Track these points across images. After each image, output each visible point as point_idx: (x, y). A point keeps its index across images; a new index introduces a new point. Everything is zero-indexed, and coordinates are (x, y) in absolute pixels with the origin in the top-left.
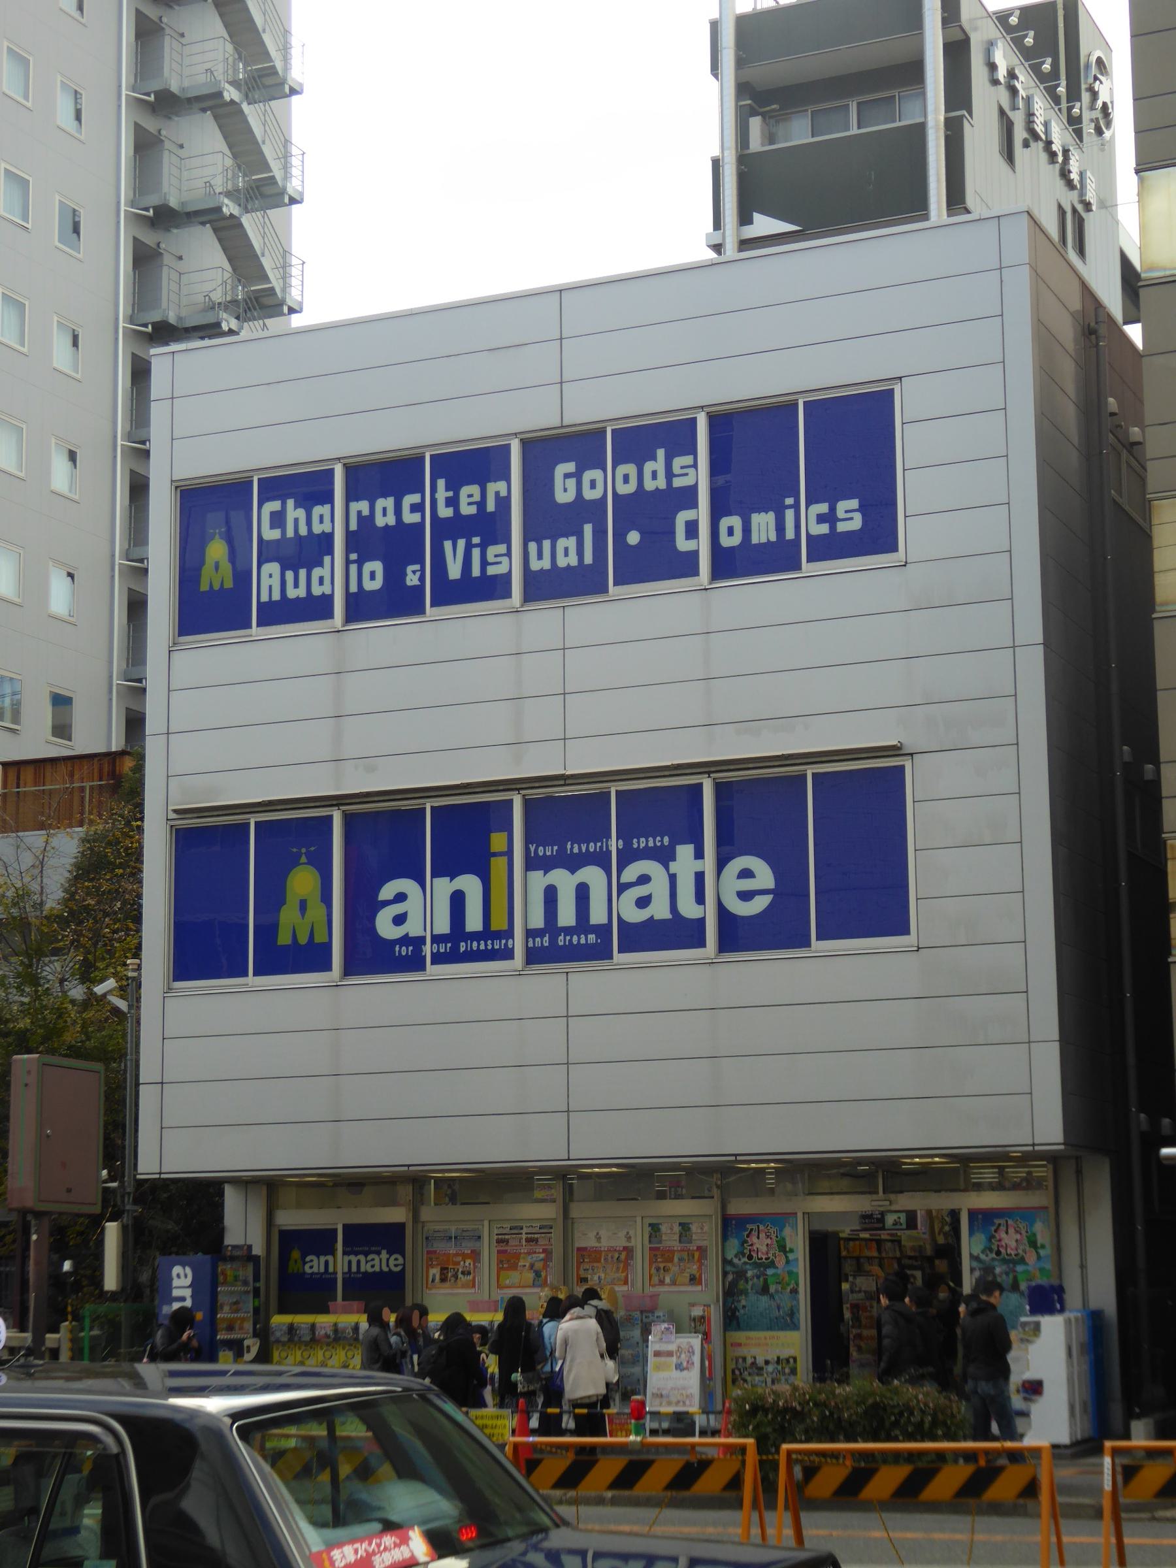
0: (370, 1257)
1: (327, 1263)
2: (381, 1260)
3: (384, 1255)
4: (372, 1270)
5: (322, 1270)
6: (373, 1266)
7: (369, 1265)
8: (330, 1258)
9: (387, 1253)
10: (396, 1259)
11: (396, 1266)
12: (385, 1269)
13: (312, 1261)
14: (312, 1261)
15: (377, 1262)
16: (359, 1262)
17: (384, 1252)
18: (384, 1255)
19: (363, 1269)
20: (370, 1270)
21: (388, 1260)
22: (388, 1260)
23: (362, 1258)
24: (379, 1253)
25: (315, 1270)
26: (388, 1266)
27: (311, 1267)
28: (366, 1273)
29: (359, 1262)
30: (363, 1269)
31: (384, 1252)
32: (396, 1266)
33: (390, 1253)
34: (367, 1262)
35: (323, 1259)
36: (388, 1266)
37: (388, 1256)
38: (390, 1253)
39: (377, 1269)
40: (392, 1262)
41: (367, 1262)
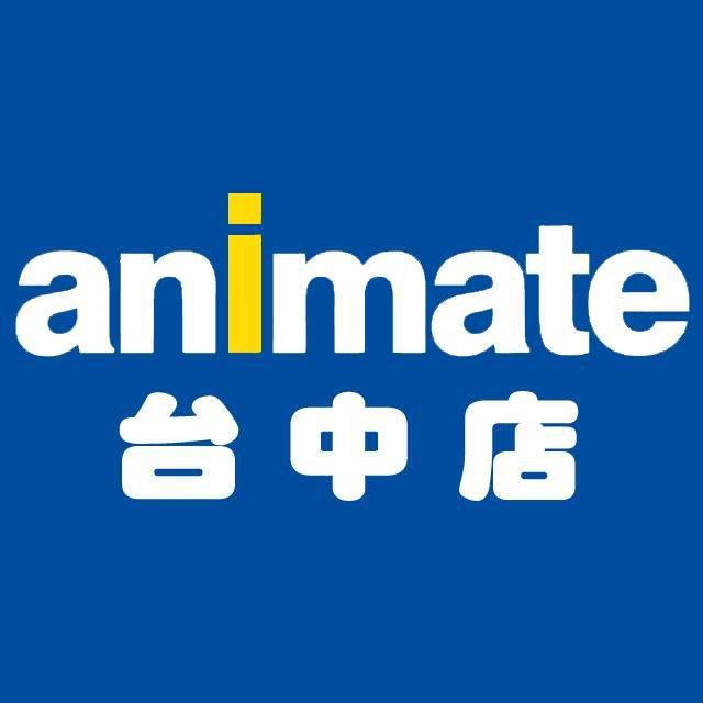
1: (168, 296)
2: (532, 283)
3: (556, 248)
6: (478, 322)
7: (453, 312)
8: (191, 269)
9: (577, 249)
11: (639, 321)
12: (564, 340)
13: (64, 283)
14: (64, 283)
15: (505, 299)
16: (379, 296)
17: (556, 239)
18: (556, 248)
19: (407, 338)
20: (459, 343)
21: (581, 285)
22: (581, 285)
23: (401, 269)
24: (521, 245)
25: (91, 337)
26: (581, 319)
27: (63, 322)
29: (379, 296)
30: (407, 338)
31: (556, 239)
32: (639, 321)
33: (596, 245)
34: (436, 296)
35: (141, 272)
36: (581, 319)
37: (582, 263)
38: (596, 245)
39: (508, 337)
41: (436, 296)
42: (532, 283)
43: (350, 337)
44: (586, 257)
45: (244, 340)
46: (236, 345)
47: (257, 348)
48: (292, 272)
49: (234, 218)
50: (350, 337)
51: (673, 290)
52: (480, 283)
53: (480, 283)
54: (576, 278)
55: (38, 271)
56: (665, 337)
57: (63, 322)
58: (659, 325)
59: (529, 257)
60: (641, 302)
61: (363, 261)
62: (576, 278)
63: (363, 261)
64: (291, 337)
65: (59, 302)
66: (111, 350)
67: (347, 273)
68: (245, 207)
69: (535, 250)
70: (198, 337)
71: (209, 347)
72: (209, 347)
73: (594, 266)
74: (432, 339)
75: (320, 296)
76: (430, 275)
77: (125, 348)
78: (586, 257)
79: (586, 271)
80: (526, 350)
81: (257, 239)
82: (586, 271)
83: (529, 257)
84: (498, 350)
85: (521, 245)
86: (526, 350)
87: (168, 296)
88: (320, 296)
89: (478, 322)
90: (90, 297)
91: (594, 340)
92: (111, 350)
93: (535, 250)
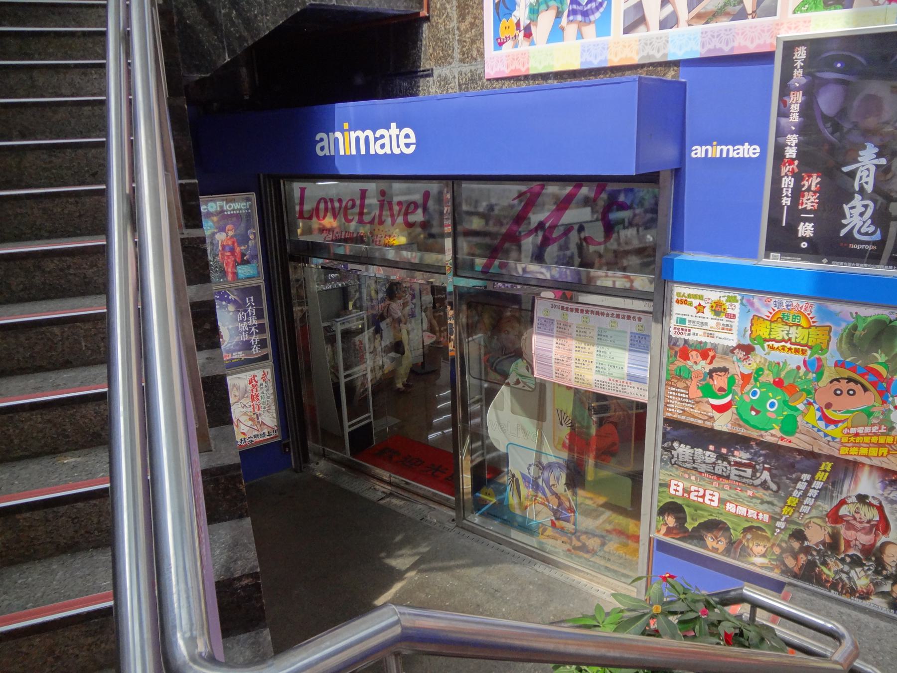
0: (736, 147)
1: (707, 151)
4: (737, 156)
5: (703, 156)
6: (738, 154)
8: (709, 147)
11: (754, 154)
12: (747, 156)
14: (696, 149)
16: (728, 150)
17: (746, 144)
19: (731, 156)
23: (730, 147)
25: (699, 155)
27: (696, 154)
28: (733, 158)
29: (728, 150)
30: (731, 156)
31: (746, 144)
32: (754, 154)
33: (751, 145)
34: (734, 150)
35: (704, 148)
39: (741, 155)
40: (751, 151)
41: (734, 150)
43: (724, 155)
45: (714, 156)
48: (719, 148)
50: (724, 155)
51: (758, 150)
52: (738, 149)
53: (738, 149)
55: (694, 148)
56: (757, 155)
57: (696, 154)
64: (718, 156)
67: (725, 148)
68: (715, 143)
70: (710, 156)
75: (722, 150)
85: (743, 145)
87: (707, 151)
88: (722, 150)
89: (738, 154)
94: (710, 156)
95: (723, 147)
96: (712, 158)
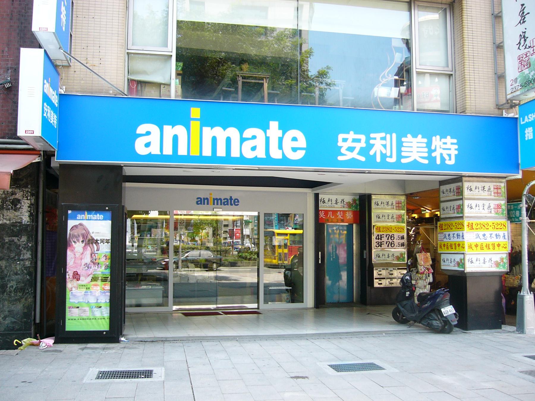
0: (248, 133)
1: (175, 138)
2: (267, 139)
6: (254, 149)
7: (247, 145)
8: (180, 130)
9: (280, 129)
10: (295, 139)
11: (295, 150)
12: (276, 154)
13: (148, 133)
14: (148, 133)
15: (260, 142)
16: (228, 141)
17: (274, 125)
19: (235, 153)
20: (249, 154)
21: (281, 140)
22: (281, 140)
24: (265, 128)
25: (155, 150)
27: (148, 145)
29: (228, 141)
30: (235, 153)
31: (274, 125)
32: (295, 150)
33: (284, 128)
34: (243, 140)
37: (280, 133)
38: (284, 128)
40: (288, 144)
42: (267, 139)
43: (221, 152)
44: (281, 131)
45: (195, 152)
46: (192, 153)
47: (198, 154)
49: (193, 116)
50: (221, 152)
51: (302, 142)
54: (279, 138)
56: (300, 155)
57: (148, 145)
58: (298, 151)
59: (268, 131)
60: (295, 144)
61: (224, 130)
62: (279, 138)
63: (224, 130)
65: (146, 139)
66: (160, 153)
69: (269, 129)
70: (182, 151)
71: (185, 153)
72: (185, 153)
73: (284, 134)
74: (242, 153)
75: (214, 140)
76: (241, 134)
77: (164, 153)
78: (281, 131)
79: (281, 136)
80: (265, 157)
81: (199, 122)
82: (281, 136)
83: (268, 131)
84: (258, 157)
85: (265, 128)
86: (265, 157)
87: (175, 138)
88: (214, 140)
89: (254, 149)
90: (155, 138)
91: (283, 153)
92: (160, 153)
93: (269, 129)
94: (182, 151)
95: (218, 131)
96: (189, 158)
